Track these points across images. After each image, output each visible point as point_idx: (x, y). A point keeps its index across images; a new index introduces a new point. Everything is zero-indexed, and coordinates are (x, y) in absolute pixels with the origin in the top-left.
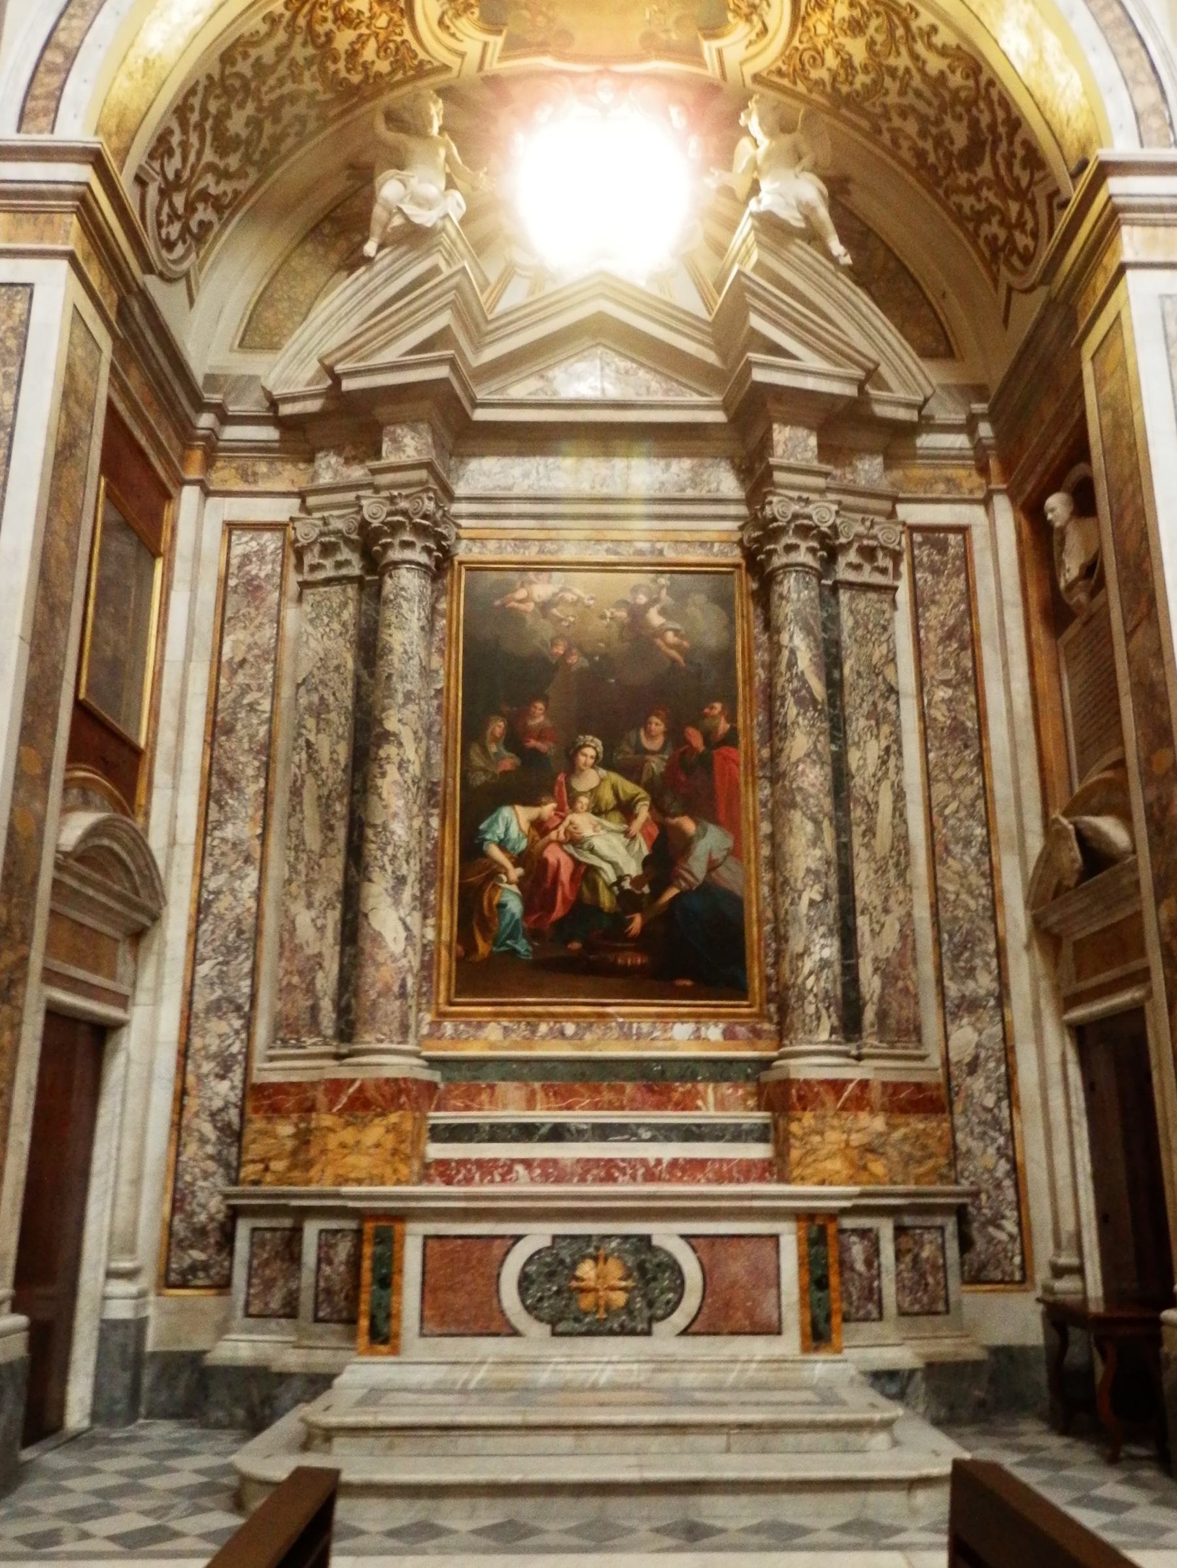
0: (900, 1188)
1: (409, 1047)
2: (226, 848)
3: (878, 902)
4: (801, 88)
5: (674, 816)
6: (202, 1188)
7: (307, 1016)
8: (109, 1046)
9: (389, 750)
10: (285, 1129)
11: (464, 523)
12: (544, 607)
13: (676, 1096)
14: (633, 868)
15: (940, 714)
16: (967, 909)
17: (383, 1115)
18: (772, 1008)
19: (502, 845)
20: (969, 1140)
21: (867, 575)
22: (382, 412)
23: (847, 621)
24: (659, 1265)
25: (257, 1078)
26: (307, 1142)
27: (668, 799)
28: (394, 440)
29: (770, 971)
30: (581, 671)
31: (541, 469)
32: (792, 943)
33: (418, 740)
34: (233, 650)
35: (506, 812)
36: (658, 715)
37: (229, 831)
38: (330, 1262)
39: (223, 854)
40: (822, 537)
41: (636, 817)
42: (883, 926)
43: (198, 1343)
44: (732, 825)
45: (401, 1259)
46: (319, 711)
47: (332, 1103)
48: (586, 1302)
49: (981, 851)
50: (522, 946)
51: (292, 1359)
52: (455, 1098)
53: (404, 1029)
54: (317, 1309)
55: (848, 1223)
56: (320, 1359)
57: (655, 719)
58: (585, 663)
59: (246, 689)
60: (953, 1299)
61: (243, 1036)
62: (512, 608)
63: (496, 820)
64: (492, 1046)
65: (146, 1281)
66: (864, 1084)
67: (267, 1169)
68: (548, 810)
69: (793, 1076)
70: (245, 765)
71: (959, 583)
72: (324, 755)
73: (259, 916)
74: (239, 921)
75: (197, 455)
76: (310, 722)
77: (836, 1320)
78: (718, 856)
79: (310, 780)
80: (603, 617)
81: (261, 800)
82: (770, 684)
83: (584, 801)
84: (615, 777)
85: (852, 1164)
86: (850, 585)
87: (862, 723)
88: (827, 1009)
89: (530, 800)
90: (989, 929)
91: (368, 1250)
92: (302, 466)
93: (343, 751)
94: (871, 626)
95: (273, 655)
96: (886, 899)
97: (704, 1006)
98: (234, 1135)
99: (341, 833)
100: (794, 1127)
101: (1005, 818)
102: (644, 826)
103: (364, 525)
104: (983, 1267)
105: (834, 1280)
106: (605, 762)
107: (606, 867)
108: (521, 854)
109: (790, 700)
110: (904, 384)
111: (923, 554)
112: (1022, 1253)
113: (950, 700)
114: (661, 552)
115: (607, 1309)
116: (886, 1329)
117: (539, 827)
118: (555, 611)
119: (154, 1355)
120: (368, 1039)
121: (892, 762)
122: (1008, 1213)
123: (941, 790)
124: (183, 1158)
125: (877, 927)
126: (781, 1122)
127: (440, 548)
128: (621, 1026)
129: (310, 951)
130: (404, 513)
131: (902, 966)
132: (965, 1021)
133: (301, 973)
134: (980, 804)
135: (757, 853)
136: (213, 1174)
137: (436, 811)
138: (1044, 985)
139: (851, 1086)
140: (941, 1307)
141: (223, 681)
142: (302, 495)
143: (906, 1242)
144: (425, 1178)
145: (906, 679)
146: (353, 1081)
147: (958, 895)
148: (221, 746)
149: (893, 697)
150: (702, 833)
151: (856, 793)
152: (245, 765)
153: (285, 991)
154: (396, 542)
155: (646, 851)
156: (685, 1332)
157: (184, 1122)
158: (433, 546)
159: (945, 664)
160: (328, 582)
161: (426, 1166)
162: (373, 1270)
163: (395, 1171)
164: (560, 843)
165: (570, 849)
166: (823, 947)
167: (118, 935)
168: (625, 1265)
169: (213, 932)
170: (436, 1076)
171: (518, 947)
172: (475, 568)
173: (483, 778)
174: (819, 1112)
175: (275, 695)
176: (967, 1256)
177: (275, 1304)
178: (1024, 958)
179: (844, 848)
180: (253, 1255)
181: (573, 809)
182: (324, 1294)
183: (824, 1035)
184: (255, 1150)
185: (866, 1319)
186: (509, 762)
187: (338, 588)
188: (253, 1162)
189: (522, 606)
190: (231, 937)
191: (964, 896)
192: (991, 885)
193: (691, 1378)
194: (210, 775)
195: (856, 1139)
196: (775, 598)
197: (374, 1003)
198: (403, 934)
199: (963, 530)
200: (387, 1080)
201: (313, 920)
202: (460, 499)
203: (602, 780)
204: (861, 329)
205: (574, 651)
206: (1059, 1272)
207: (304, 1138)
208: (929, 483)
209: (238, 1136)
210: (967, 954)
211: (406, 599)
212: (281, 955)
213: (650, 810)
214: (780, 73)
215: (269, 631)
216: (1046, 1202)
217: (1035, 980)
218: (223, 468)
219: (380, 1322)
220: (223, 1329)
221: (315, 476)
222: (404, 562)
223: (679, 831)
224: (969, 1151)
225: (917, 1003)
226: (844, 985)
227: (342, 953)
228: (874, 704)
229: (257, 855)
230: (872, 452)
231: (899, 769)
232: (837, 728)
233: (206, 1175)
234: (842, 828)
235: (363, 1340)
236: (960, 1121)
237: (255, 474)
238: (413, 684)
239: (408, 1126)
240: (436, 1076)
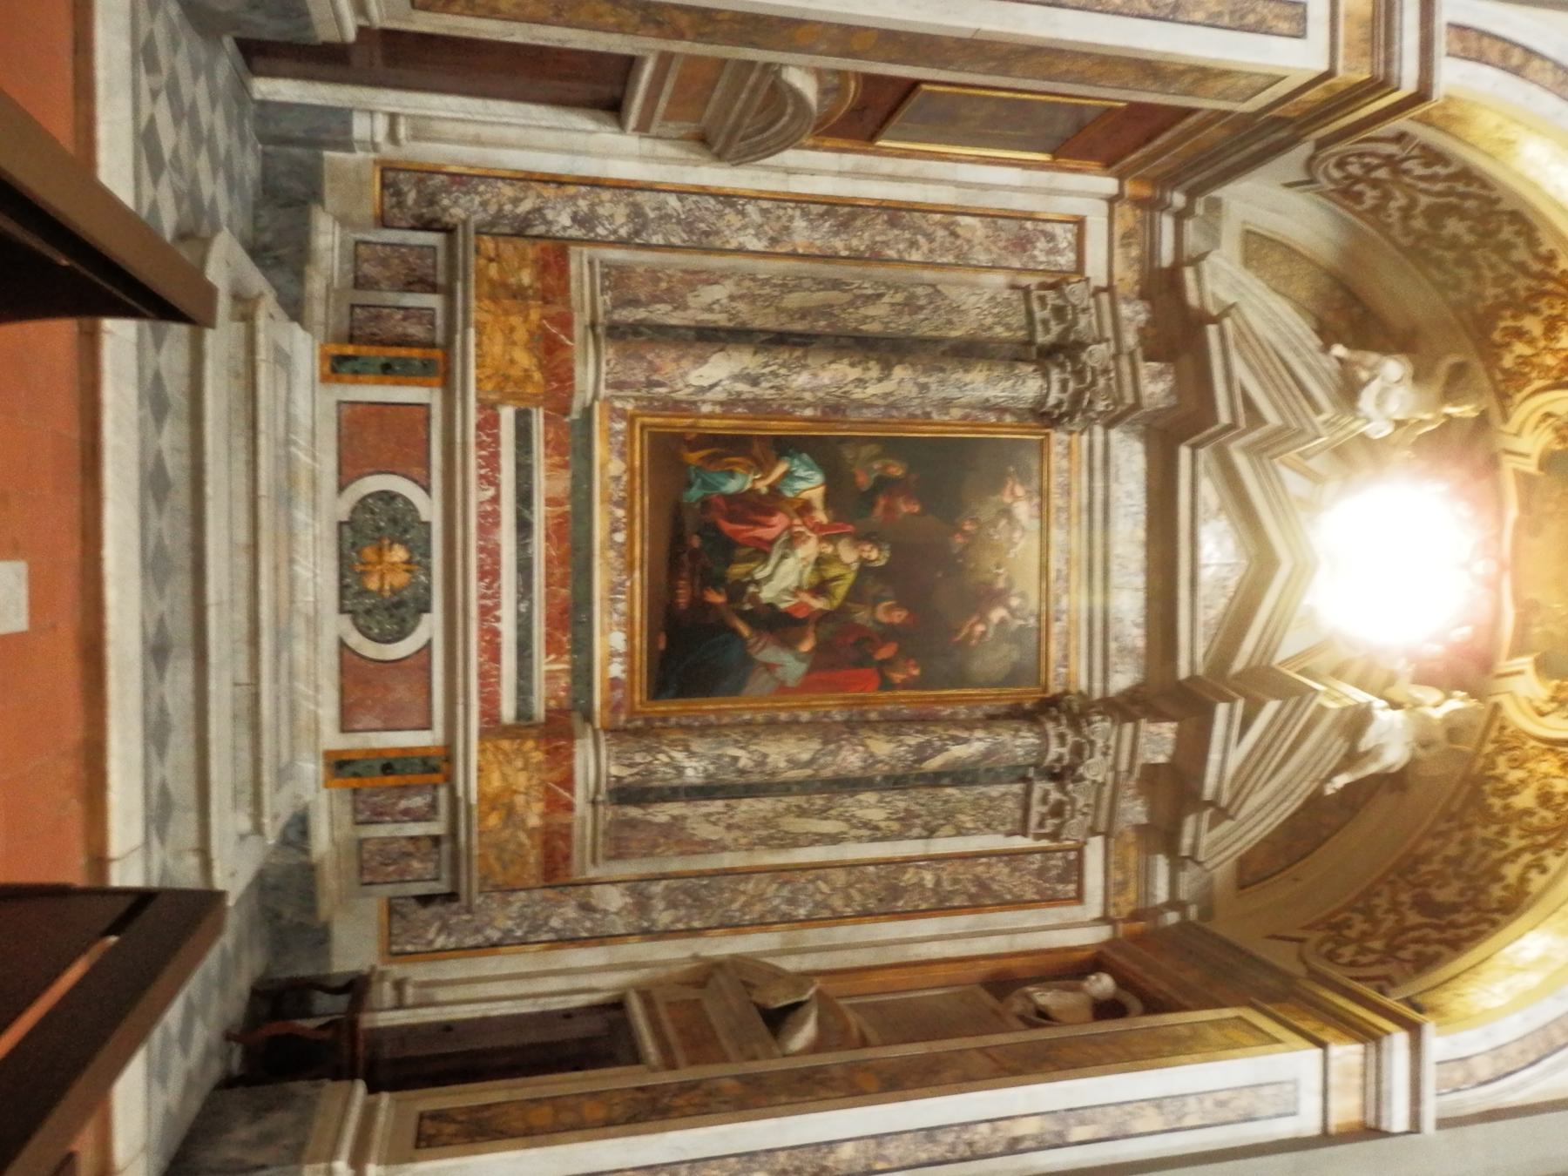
0: (475, 840)
1: (603, 391)
2: (784, 219)
3: (735, 820)
4: (1489, 748)
6: (472, 201)
7: (630, 297)
8: (601, 114)
9: (875, 371)
10: (526, 277)
11: (1085, 438)
12: (1007, 512)
13: (558, 635)
14: (767, 594)
15: (909, 876)
16: (731, 901)
17: (541, 367)
18: (639, 723)
19: (788, 475)
20: (519, 904)
21: (1037, 809)
22: (1186, 361)
23: (995, 791)
24: (403, 620)
25: (574, 250)
26: (515, 297)
28: (1161, 373)
29: (673, 721)
31: (1134, 509)
32: (699, 741)
33: (886, 395)
34: (967, 226)
35: (818, 478)
36: (908, 617)
37: (800, 224)
38: (405, 319)
39: (779, 218)
40: (1072, 768)
42: (715, 824)
43: (331, 200)
44: (806, 686)
45: (408, 384)
46: (910, 305)
47: (552, 320)
48: (369, 553)
49: (784, 914)
50: (695, 494)
51: (316, 285)
52: (556, 433)
53: (618, 385)
54: (363, 306)
55: (443, 793)
56: (317, 311)
59: (930, 238)
60: (375, 889)
61: (612, 238)
62: (1006, 483)
64: (603, 466)
65: (387, 150)
66: (569, 807)
67: (491, 260)
68: (821, 516)
69: (578, 743)
70: (861, 238)
71: (1030, 894)
72: (871, 311)
73: (722, 251)
74: (717, 233)
75: (1146, 192)
76: (900, 297)
77: (354, 782)
78: (779, 672)
79: (846, 297)
80: (998, 566)
81: (829, 252)
82: (937, 720)
83: (829, 549)
84: (851, 577)
85: (497, 796)
86: (1028, 793)
87: (902, 805)
88: (637, 774)
89: (829, 500)
90: (712, 922)
91: (416, 353)
92: (1137, 288)
93: (873, 328)
94: (991, 812)
95: (962, 263)
96: (739, 827)
97: (641, 660)
98: (520, 230)
99: (799, 326)
100: (530, 744)
101: (813, 936)
102: (806, 605)
103: (1081, 345)
104: (403, 916)
105: (391, 780)
106: (865, 568)
108: (779, 491)
109: (922, 738)
110: (1214, 843)
111: (1057, 861)
112: (416, 953)
113: (923, 886)
114: (1058, 619)
115: (363, 573)
116: (346, 829)
117: (805, 508)
119: (321, 158)
120: (609, 353)
121: (865, 832)
122: (453, 939)
123: (840, 877)
124: (500, 184)
125: (713, 819)
126: (534, 732)
127: (1062, 416)
128: (622, 584)
129: (691, 300)
130: (1094, 383)
131: (678, 842)
132: (629, 900)
133: (669, 290)
134: (826, 913)
135: (780, 709)
136: (485, 210)
137: (819, 413)
138: (662, 972)
139: (567, 795)
140: (367, 878)
141: (938, 217)
142: (1110, 289)
143: (426, 846)
144: (483, 405)
145: (944, 845)
146: (571, 338)
147: (744, 893)
148: (879, 214)
149: (925, 833)
150: (800, 658)
151: (838, 800)
152: (861, 238)
153: (653, 275)
154: (1067, 376)
155: (783, 606)
156: (342, 645)
157: (533, 184)
158: (1064, 409)
159: (955, 881)
160: (1030, 313)
161: (493, 406)
162: (398, 358)
163: (489, 377)
165: (784, 538)
166: (695, 768)
167: (704, 123)
168: (404, 588)
169: (707, 209)
170: (575, 416)
172: (1042, 449)
174: (544, 767)
175: (925, 265)
176: (412, 901)
177: (368, 269)
178: (687, 954)
179: (786, 788)
180: (411, 247)
181: (822, 540)
182: (377, 313)
183: (614, 770)
184: (507, 249)
185: (356, 811)
186: (864, 481)
187: (1024, 321)
188: (497, 248)
189: (1007, 492)
190: (703, 226)
191: (743, 899)
192: (752, 925)
193: (301, 650)
194: (852, 206)
195: (520, 800)
196: (1015, 725)
197: (642, 358)
198: (706, 383)
199: (1079, 898)
200: (571, 370)
201: (718, 301)
202: (1106, 434)
203: (848, 566)
204: (1264, 805)
206: (399, 985)
207: (518, 294)
208: (1122, 866)
209: (519, 234)
210: (689, 901)
211: (1013, 386)
212: (685, 271)
213: (821, 610)
214: (1503, 728)
215: (983, 258)
216: (463, 974)
217: (665, 964)
218: (1135, 216)
219: (349, 365)
220: (343, 221)
221: (1128, 300)
222: (1049, 383)
223: (800, 639)
224: (509, 903)
225: (645, 855)
226: (660, 789)
227: (688, 328)
228: (919, 816)
229: (778, 249)
230: (1151, 813)
231: (859, 839)
232: (896, 782)
233: (484, 204)
234: (805, 787)
235: (334, 350)
236: (537, 895)
237: (1129, 245)
238: (936, 392)
239: (530, 390)
240: (575, 415)
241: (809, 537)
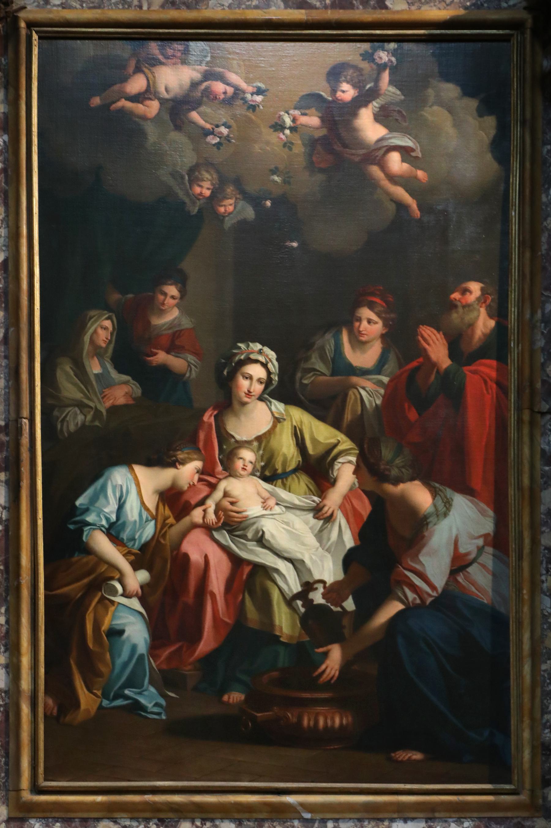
5: (397, 481)
27: (387, 453)
36: (371, 306)
41: (333, 483)
57: (366, 313)
58: (250, 213)
62: (122, 110)
63: (104, 489)
80: (279, 127)
102: (347, 498)
108: (144, 547)
118: (194, 116)
155: (349, 542)
164: (208, 529)
165: (224, 537)
173: (80, 418)
181: (230, 472)
189: (139, 108)
203: (277, 420)
205: (230, 189)
241: (226, 494)
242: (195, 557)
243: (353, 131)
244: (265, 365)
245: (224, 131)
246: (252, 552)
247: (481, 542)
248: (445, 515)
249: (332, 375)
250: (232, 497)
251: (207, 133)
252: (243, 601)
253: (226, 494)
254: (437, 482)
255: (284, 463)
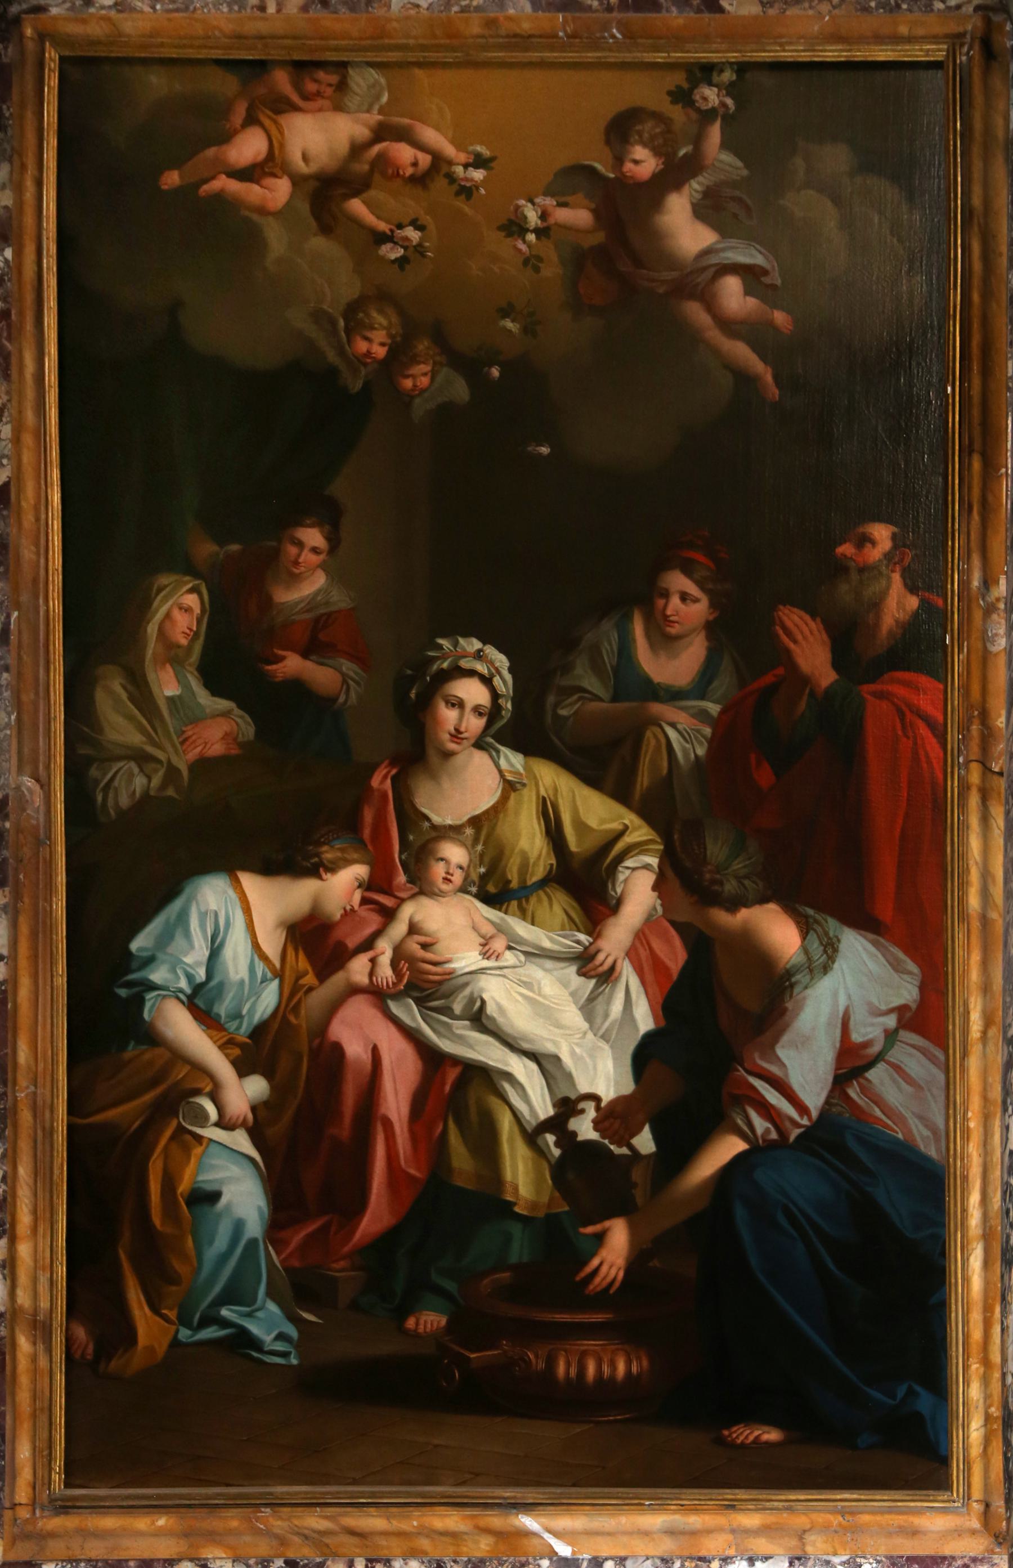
5: (734, 905)
27: (716, 850)
30: (446, 412)
41: (615, 907)
58: (460, 390)
62: (219, 197)
63: (183, 918)
80: (516, 227)
83: (455, 853)
102: (641, 936)
107: (520, 1068)
108: (259, 1031)
118: (356, 206)
155: (645, 1021)
165: (409, 1012)
171: (254, 1329)
173: (139, 782)
189: (252, 192)
203: (510, 787)
205: (423, 346)
241: (413, 929)
242: (355, 1049)
243: (656, 237)
244: (487, 681)
245: (413, 235)
246: (461, 1039)
247: (891, 1021)
248: (826, 969)
249: (615, 699)
250: (426, 935)
251: (382, 238)
252: (445, 1132)
253: (413, 929)
254: (812, 907)
255: (524, 868)
